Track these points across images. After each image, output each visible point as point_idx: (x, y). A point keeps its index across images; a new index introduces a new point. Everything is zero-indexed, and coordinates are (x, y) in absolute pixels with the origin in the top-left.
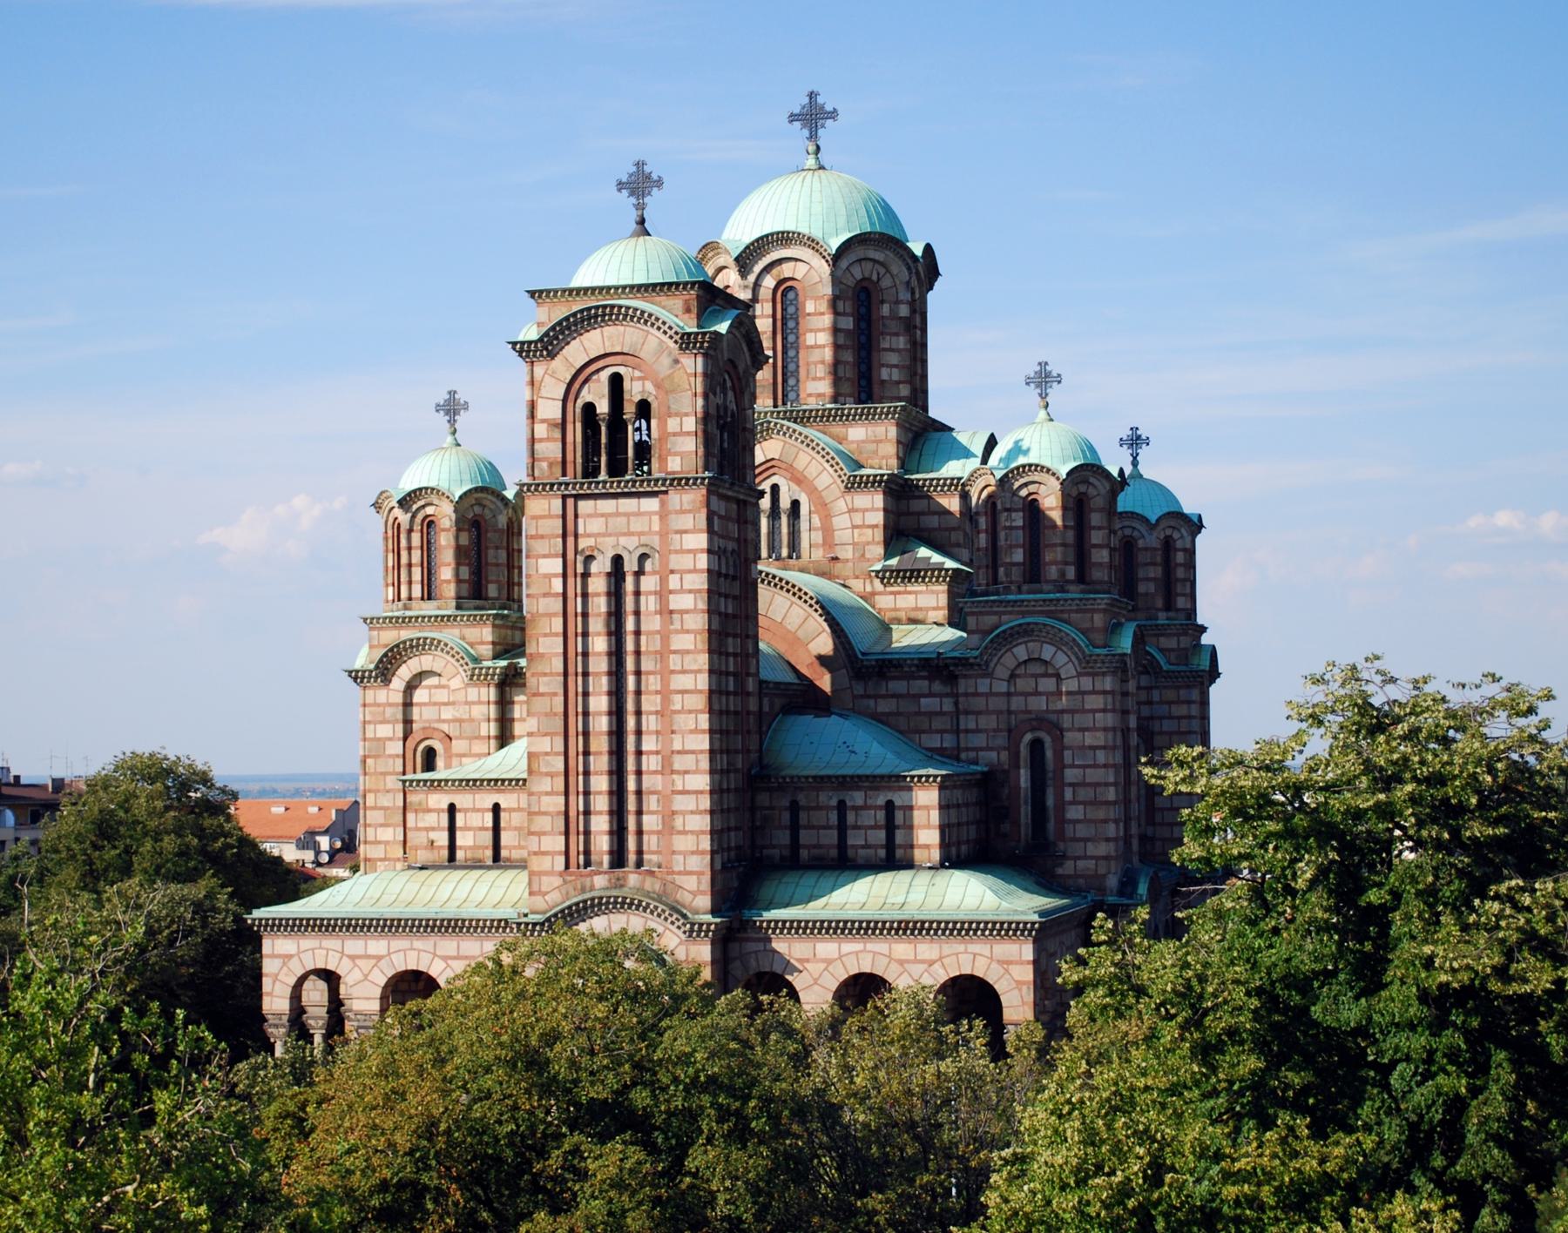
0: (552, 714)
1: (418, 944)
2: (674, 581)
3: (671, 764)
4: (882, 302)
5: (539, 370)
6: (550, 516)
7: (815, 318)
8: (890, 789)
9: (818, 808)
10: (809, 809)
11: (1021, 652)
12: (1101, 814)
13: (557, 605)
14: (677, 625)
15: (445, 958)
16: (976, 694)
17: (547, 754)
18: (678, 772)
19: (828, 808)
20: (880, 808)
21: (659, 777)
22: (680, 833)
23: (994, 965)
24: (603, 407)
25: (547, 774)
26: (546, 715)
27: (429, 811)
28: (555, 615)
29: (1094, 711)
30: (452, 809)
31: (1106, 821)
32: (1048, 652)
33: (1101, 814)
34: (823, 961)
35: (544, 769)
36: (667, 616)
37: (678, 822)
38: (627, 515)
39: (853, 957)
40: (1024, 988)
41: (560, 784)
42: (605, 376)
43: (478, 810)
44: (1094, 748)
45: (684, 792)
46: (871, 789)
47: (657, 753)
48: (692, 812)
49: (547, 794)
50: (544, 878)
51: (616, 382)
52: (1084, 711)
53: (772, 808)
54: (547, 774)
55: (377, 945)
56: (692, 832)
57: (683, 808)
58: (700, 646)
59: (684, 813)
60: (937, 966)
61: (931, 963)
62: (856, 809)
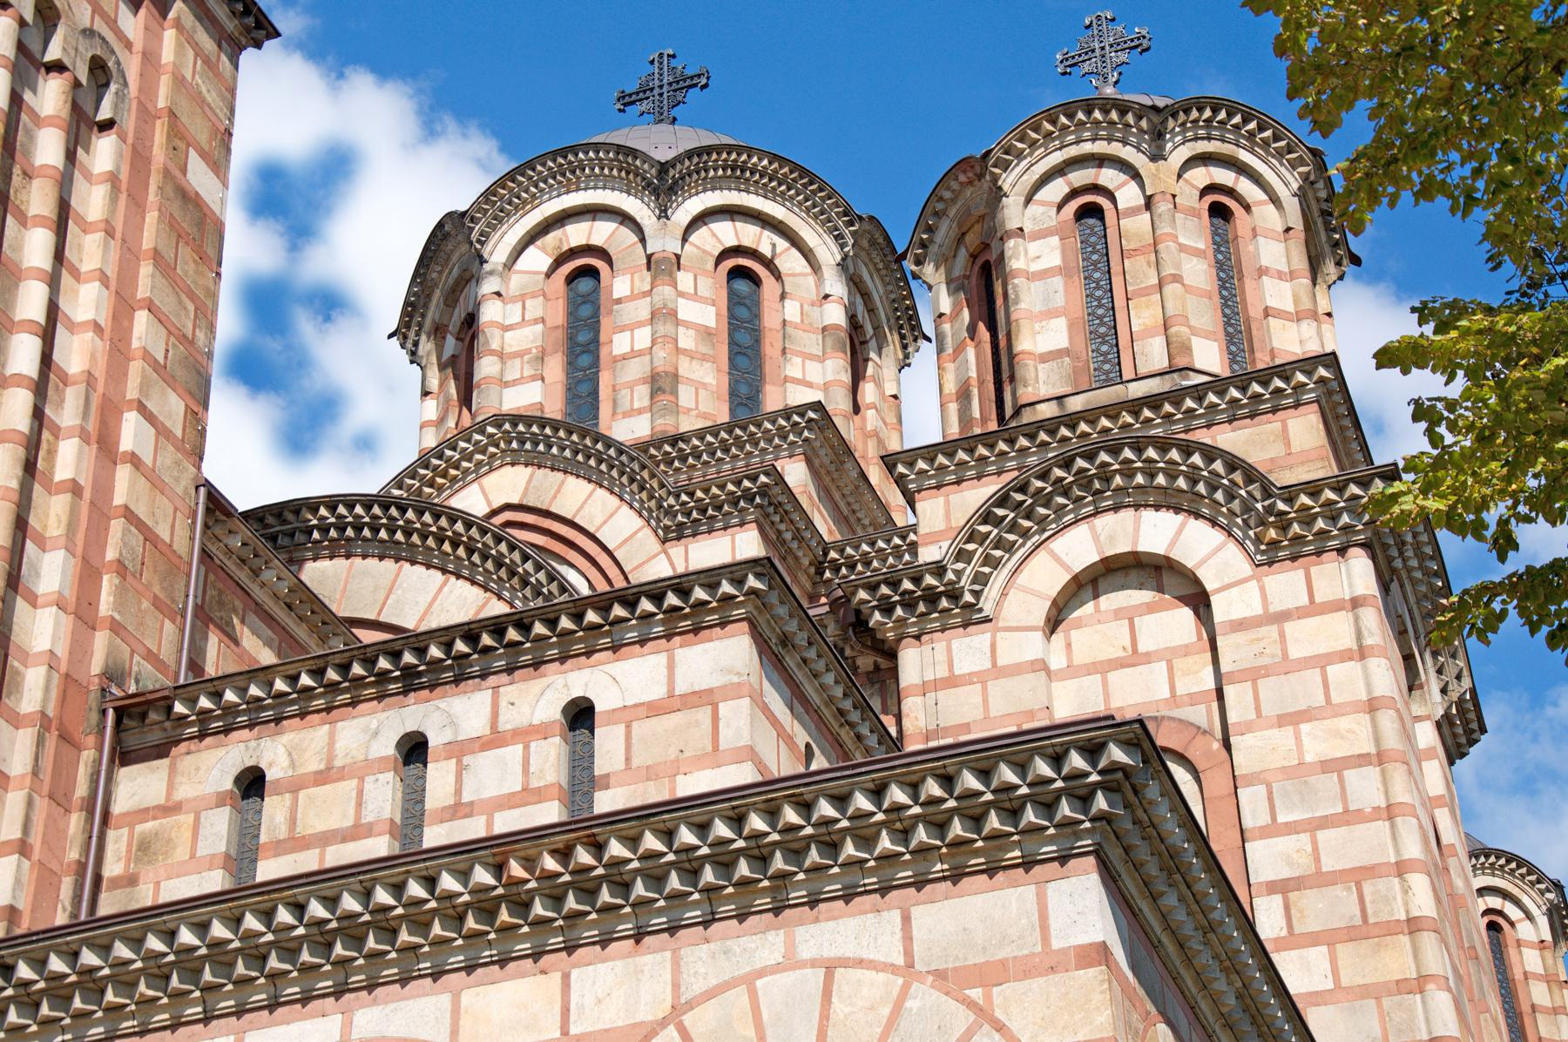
4: (783, 296)
7: (630, 306)
9: (324, 777)
10: (295, 786)
11: (1080, 546)
12: (1396, 960)
16: (952, 681)
19: (361, 770)
20: (541, 731)
23: (924, 998)
29: (1322, 662)
31: (1419, 984)
32: (1156, 532)
33: (1396, 960)
44: (1334, 766)
52: (1287, 666)
53: (170, 809)
62: (459, 750)
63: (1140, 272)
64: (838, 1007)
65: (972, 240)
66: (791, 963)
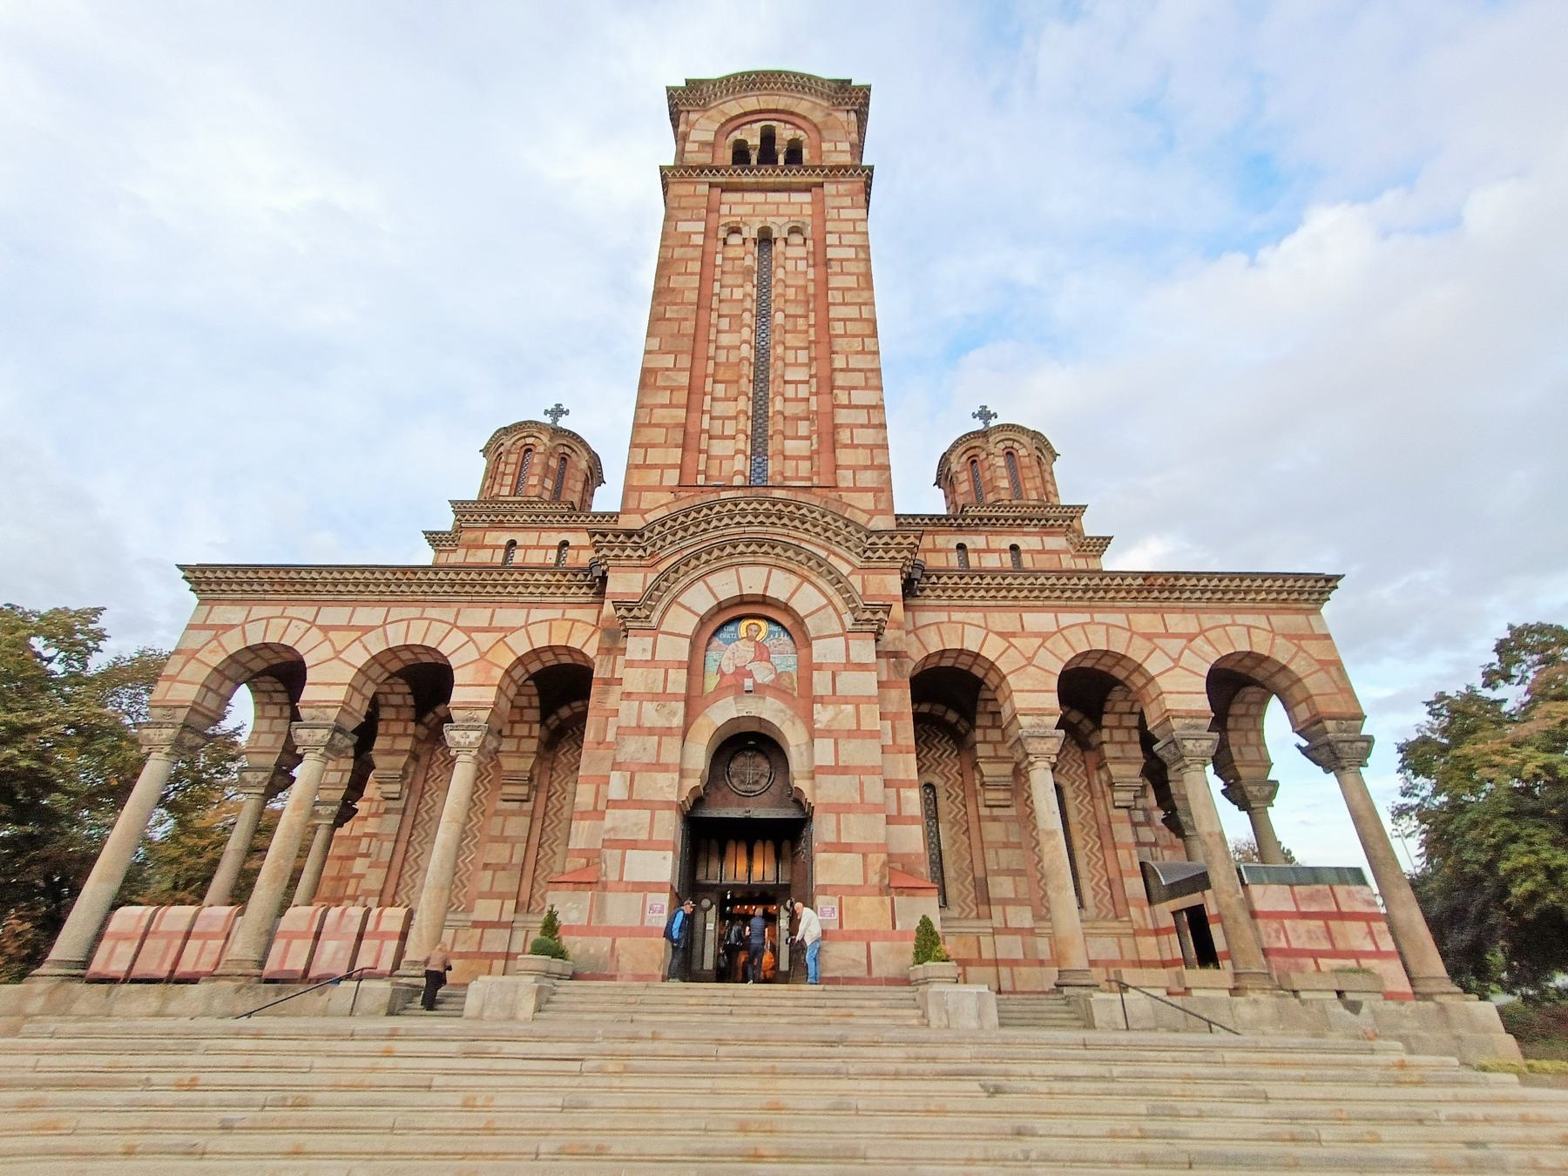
0: (679, 335)
1: (432, 612)
2: (831, 239)
3: (831, 380)
5: (693, 116)
6: (695, 195)
8: (1012, 533)
13: (698, 253)
14: (836, 267)
15: (468, 631)
17: (667, 369)
18: (842, 388)
19: (947, 551)
20: (1004, 551)
21: (813, 399)
22: (846, 446)
23: (1279, 641)
24: (755, 141)
25: (665, 388)
26: (672, 336)
27: (486, 547)
28: (692, 260)
30: (512, 543)
34: (1037, 635)
35: (660, 383)
36: (821, 269)
37: (844, 436)
38: (778, 204)
39: (1078, 630)
40: (1333, 669)
41: (681, 397)
42: (757, 127)
43: (542, 547)
45: (849, 406)
46: (992, 533)
47: (807, 382)
48: (862, 426)
49: (663, 406)
50: (647, 495)
51: (768, 137)
54: (665, 388)
55: (364, 616)
56: (864, 446)
57: (849, 421)
58: (862, 284)
59: (852, 427)
60: (1199, 641)
61: (1191, 638)
63: (1027, 473)
64: (1254, 639)
65: (971, 453)
66: (1234, 624)
